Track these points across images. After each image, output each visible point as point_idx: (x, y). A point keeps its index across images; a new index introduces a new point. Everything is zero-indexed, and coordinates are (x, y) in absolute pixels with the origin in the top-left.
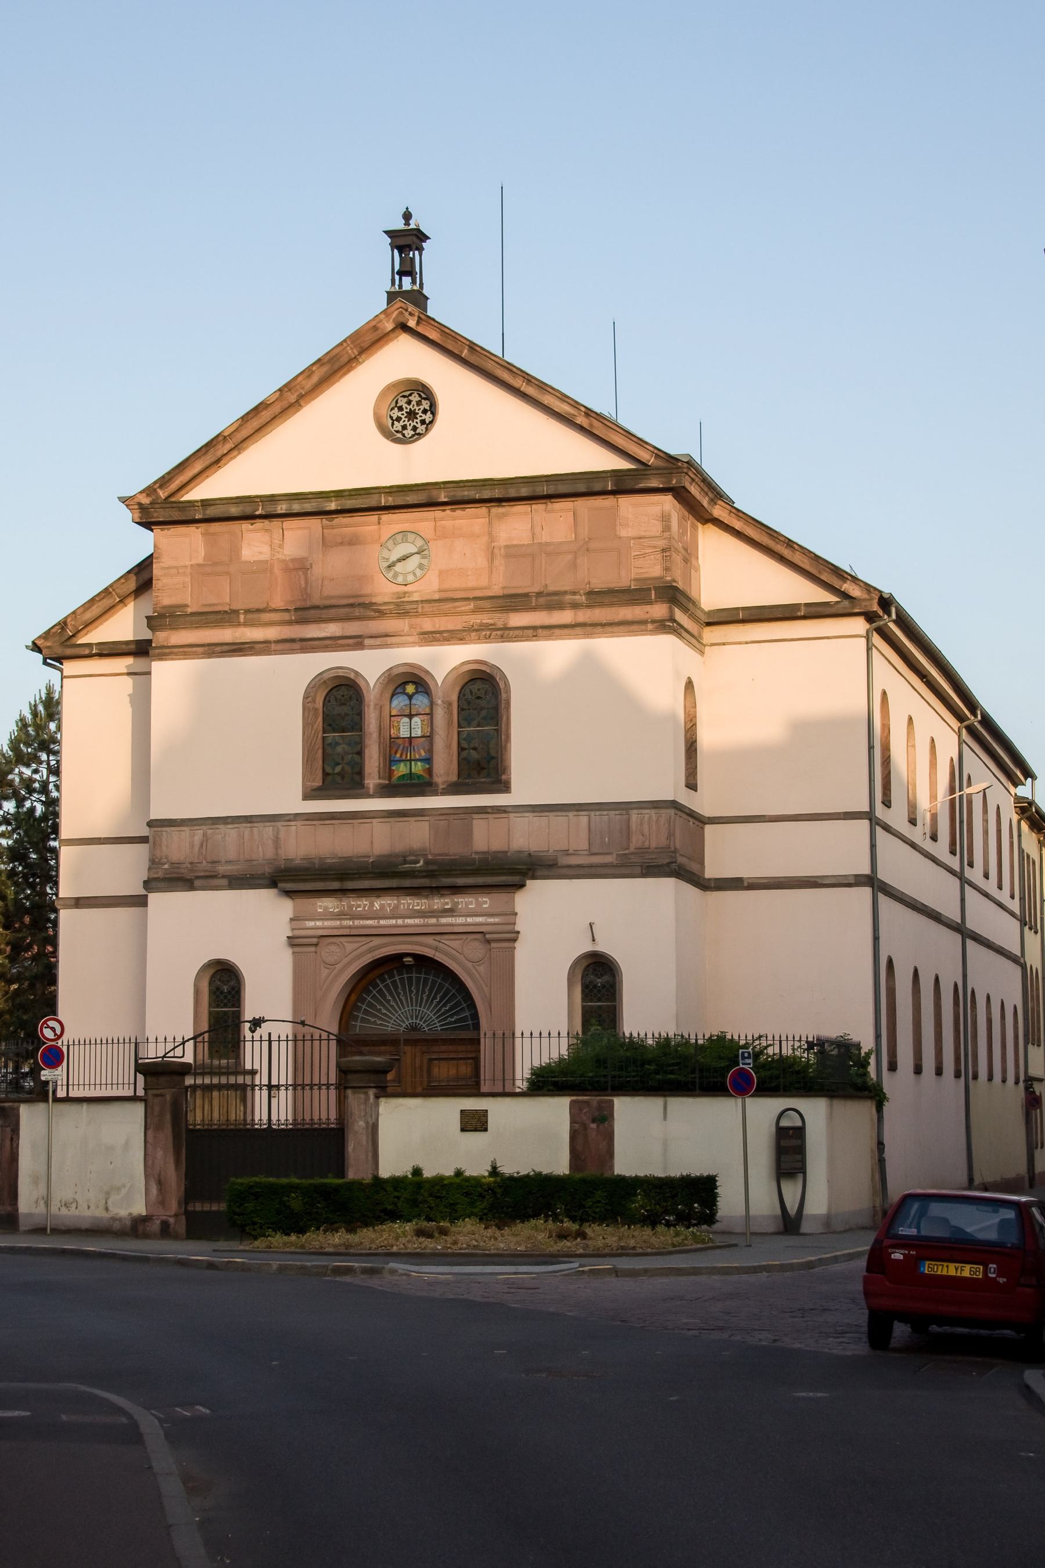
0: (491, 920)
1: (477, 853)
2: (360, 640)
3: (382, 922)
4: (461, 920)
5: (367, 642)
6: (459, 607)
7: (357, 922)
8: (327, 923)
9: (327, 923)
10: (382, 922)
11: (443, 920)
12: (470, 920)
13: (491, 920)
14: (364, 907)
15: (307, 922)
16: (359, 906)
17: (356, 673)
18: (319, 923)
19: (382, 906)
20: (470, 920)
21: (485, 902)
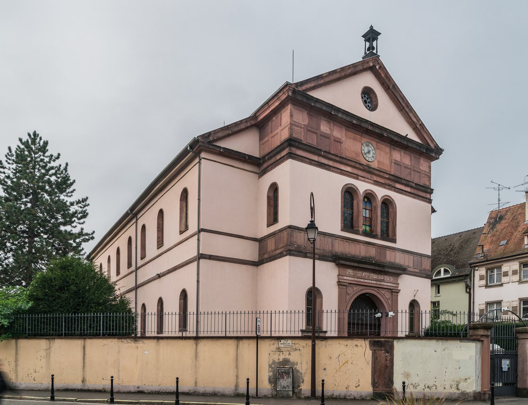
0: (393, 285)
1: (387, 262)
2: (358, 176)
3: (366, 281)
4: (386, 284)
5: (360, 178)
6: (385, 175)
7: (359, 279)
8: (350, 279)
9: (350, 279)
10: (366, 281)
11: (382, 283)
12: (388, 284)
13: (393, 285)
14: (360, 275)
15: (344, 277)
16: (359, 274)
17: (357, 188)
18: (348, 278)
19: (365, 275)
20: (388, 284)
21: (391, 279)
